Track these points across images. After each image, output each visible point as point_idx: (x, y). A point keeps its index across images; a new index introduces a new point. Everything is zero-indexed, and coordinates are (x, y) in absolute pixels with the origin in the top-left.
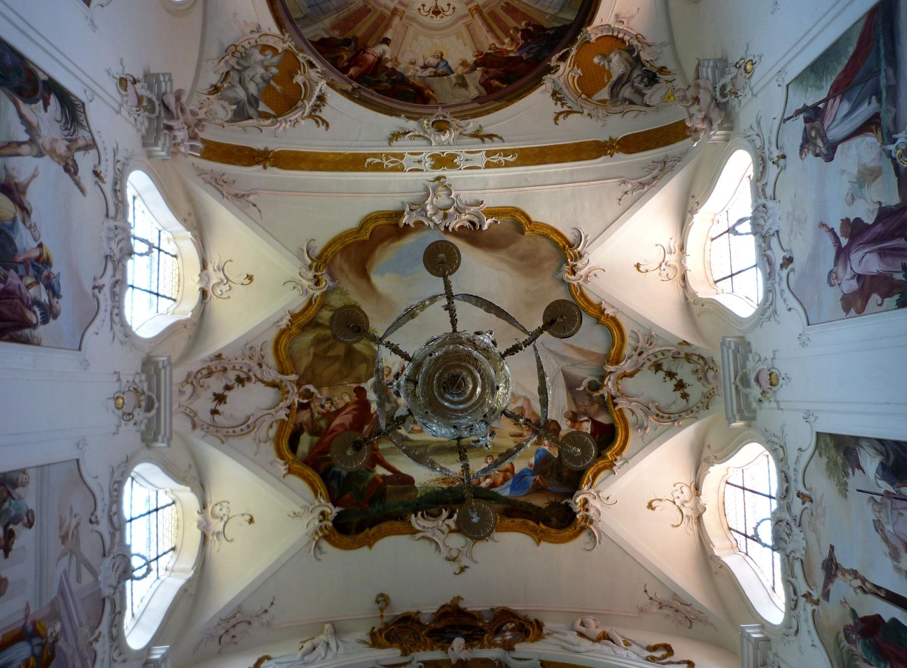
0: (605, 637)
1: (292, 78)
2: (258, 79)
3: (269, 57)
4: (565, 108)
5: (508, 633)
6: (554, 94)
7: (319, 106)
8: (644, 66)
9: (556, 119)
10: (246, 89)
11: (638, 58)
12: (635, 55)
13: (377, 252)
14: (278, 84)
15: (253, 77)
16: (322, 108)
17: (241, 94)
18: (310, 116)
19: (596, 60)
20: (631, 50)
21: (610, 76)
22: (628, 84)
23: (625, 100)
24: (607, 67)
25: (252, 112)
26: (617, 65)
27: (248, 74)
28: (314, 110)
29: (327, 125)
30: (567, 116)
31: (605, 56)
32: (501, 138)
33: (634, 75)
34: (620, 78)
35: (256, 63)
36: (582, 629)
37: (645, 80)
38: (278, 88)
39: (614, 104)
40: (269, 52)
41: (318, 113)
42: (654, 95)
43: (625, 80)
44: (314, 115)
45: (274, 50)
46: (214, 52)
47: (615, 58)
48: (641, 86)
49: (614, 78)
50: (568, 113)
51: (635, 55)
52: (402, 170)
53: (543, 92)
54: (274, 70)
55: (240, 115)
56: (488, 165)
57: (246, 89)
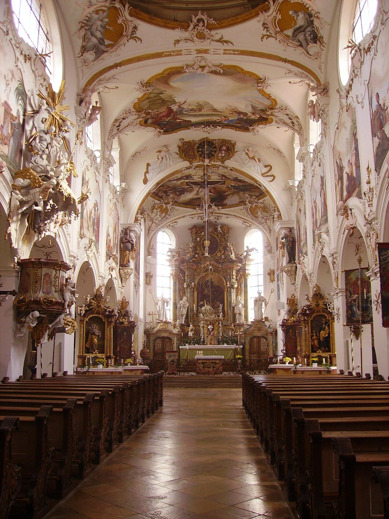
0: (253, 158)
1: (117, 21)
2: (100, 28)
3: (101, 14)
4: (268, 33)
5: (223, 152)
6: (264, 24)
7: (134, 31)
8: (314, 27)
9: (262, 38)
10: (96, 37)
11: (312, 22)
12: (312, 19)
13: (172, 78)
14: (110, 26)
15: (97, 28)
16: (137, 32)
17: (94, 40)
18: (131, 38)
19: (291, 13)
20: (310, 16)
21: (295, 24)
22: (303, 33)
23: (299, 41)
24: (295, 18)
25: (103, 48)
26: (301, 20)
27: (94, 27)
28: (133, 34)
29: (141, 40)
30: (268, 38)
31: (296, 12)
32: (232, 44)
33: (308, 30)
34: (300, 27)
35: (95, 20)
36: (247, 152)
37: (312, 36)
38: (111, 28)
39: (293, 40)
40: (100, 12)
41: (135, 35)
42: (313, 48)
43: (302, 29)
44: (133, 36)
45: (104, 11)
46: (74, 27)
47: (301, 15)
48: (309, 38)
49: (297, 26)
50: (269, 36)
51: (312, 19)
52: (181, 54)
53: (259, 21)
54: (106, 20)
55: (99, 53)
56: (224, 54)
57: (96, 37)
